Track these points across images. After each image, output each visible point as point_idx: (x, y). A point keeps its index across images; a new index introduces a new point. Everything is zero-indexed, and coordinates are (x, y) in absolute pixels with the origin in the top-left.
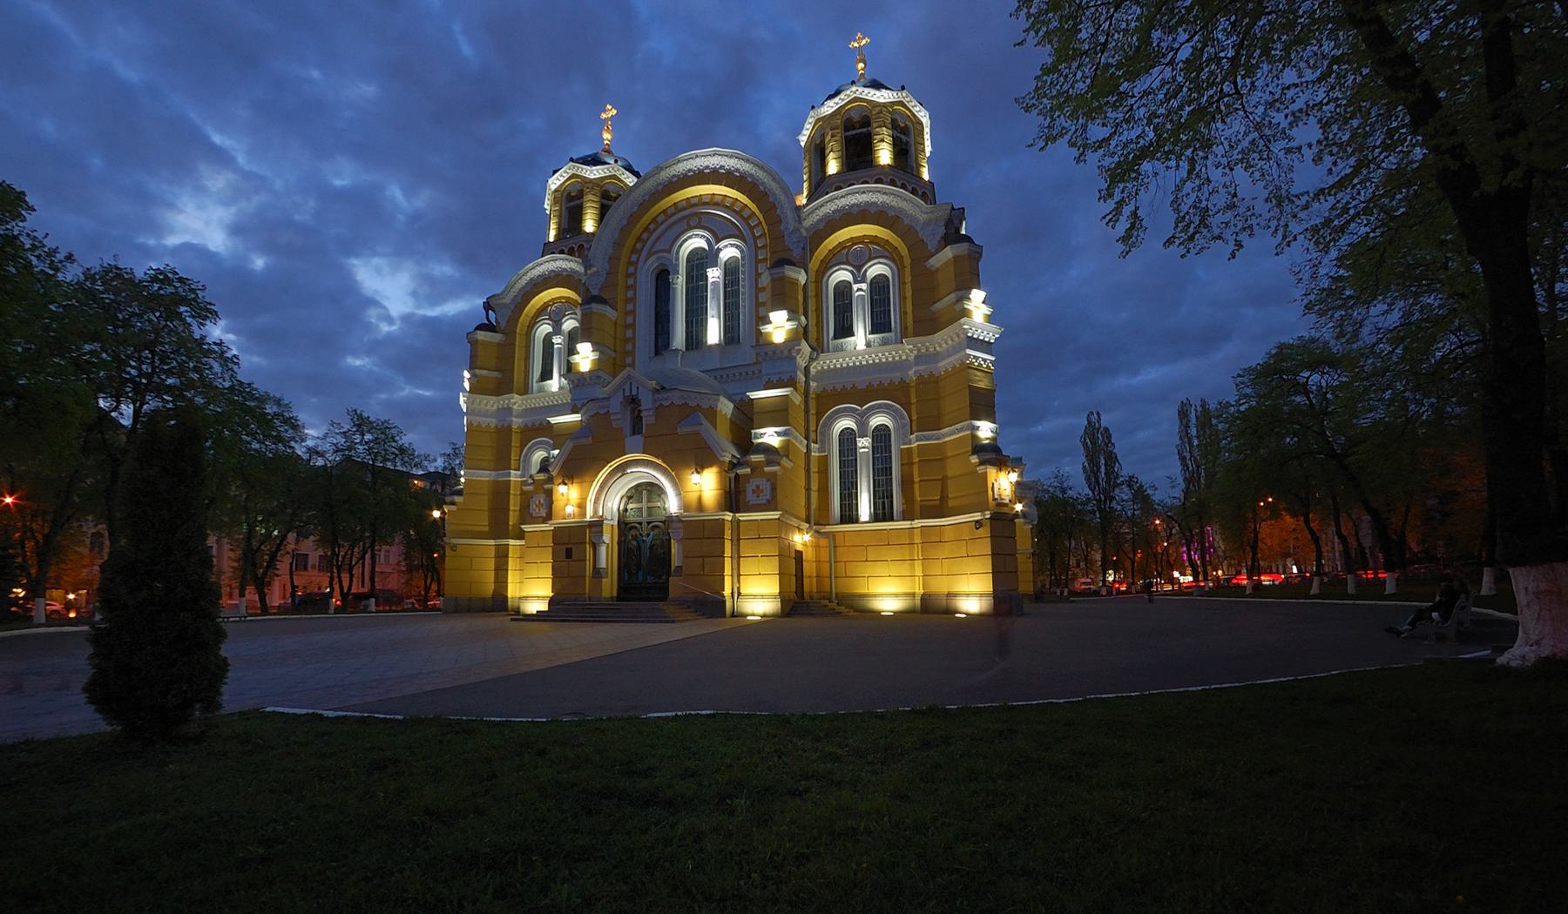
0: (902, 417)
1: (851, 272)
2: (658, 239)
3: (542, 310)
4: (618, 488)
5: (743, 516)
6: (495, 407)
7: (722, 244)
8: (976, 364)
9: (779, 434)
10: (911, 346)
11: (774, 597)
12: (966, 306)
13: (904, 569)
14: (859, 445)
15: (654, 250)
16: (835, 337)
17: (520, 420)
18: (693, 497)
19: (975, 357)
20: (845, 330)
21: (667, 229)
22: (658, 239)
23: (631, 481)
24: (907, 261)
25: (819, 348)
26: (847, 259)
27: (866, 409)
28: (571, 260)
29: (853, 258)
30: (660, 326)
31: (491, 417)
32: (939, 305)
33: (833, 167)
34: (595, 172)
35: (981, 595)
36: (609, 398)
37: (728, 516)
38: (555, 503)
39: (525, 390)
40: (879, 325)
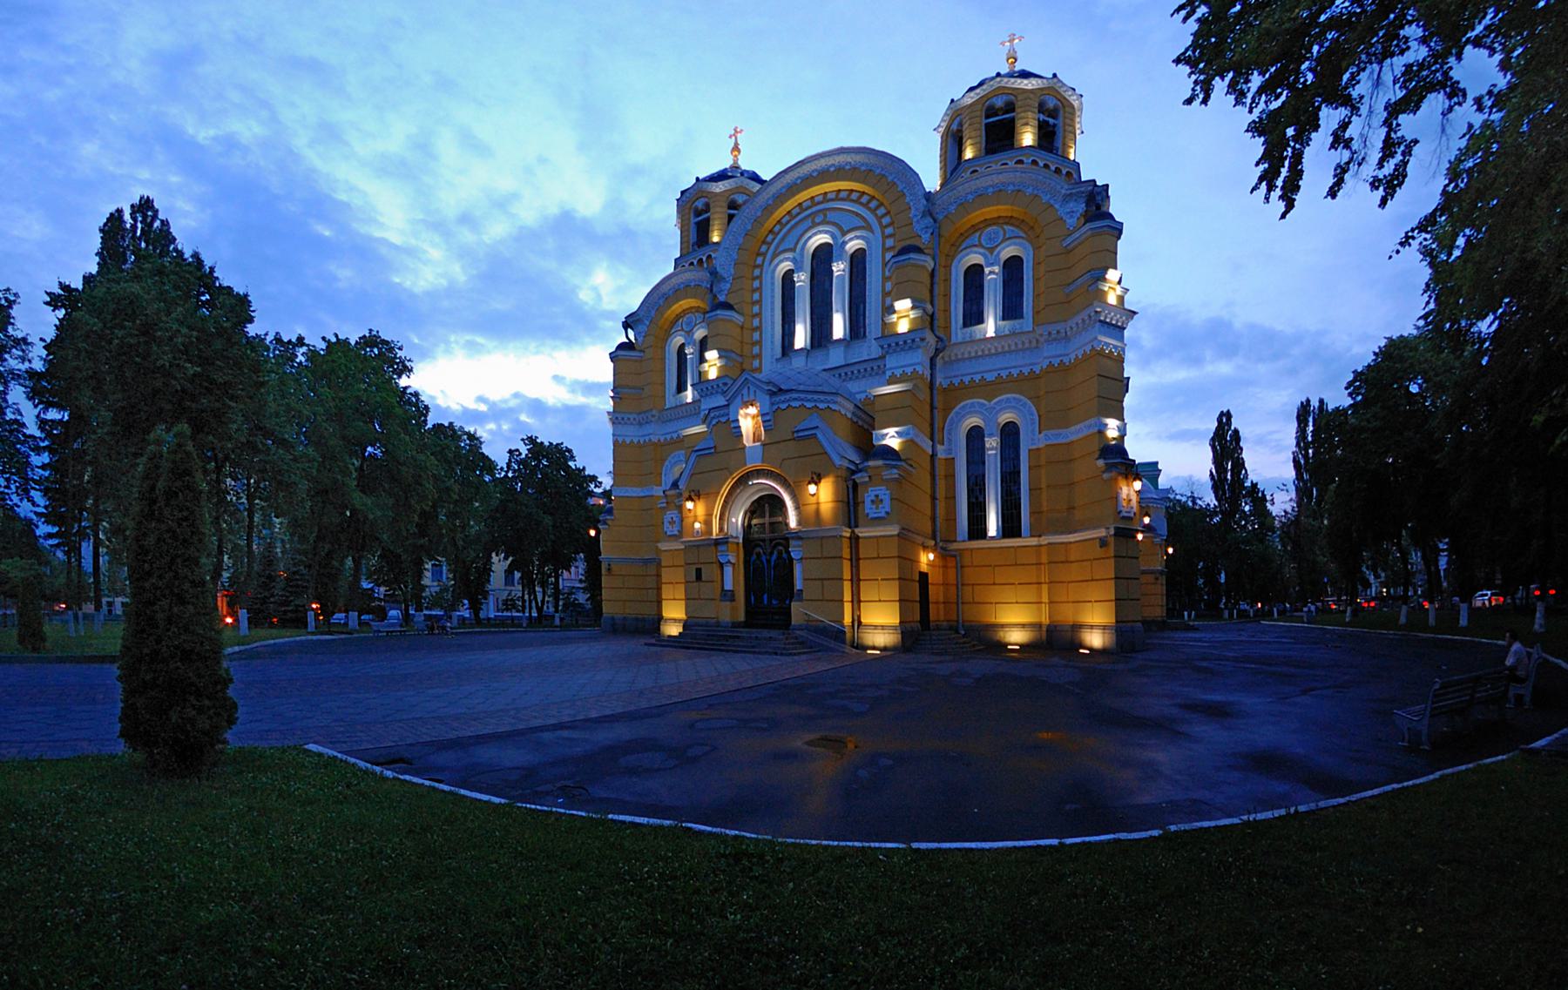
2: (783, 239)
4: (744, 498)
7: (848, 237)
12: (1100, 287)
13: (1029, 594)
14: (987, 445)
15: (781, 249)
16: (965, 325)
19: (1106, 343)
20: (974, 316)
21: (789, 231)
22: (783, 239)
23: (753, 494)
26: (979, 241)
30: (787, 326)
35: (1104, 628)
36: (728, 405)
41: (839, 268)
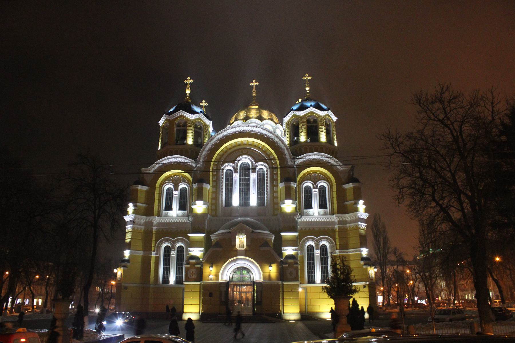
0: (332, 243)
1: (313, 184)
3: (167, 179)
5: (285, 283)
6: (144, 221)
7: (258, 164)
8: (361, 227)
9: (293, 250)
10: (337, 217)
11: (298, 313)
17: (156, 228)
18: (267, 274)
24: (334, 183)
25: (302, 214)
26: (310, 178)
27: (319, 239)
28: (187, 159)
29: (315, 179)
31: (142, 225)
32: (347, 203)
33: (303, 138)
34: (193, 117)
37: (280, 283)
38: (203, 273)
39: (159, 215)
40: (323, 206)
41: (254, 176)
